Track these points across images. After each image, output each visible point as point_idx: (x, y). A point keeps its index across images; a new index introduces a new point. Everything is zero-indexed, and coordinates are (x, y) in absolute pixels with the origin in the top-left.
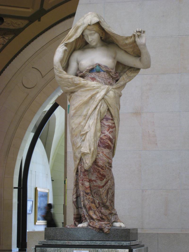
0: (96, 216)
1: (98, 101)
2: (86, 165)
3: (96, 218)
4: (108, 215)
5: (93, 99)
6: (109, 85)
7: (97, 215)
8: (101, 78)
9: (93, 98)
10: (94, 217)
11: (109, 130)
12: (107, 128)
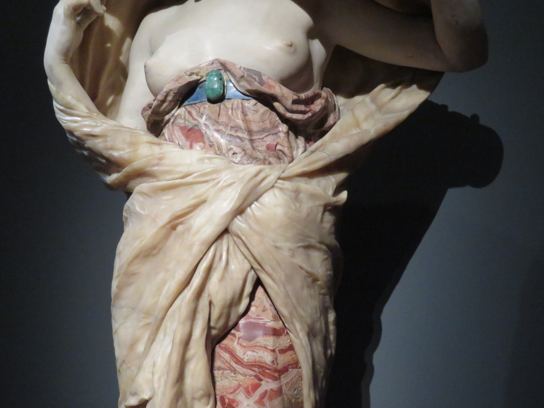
1: (196, 249)
5: (183, 233)
6: (272, 160)
8: (228, 132)
9: (180, 228)
11: (256, 387)
12: (245, 377)
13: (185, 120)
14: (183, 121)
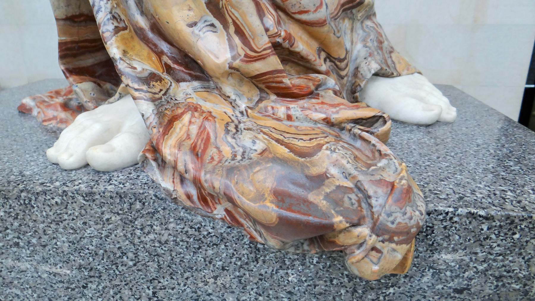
0: (237, 40)
3: (237, 63)
4: (335, 18)
7: (239, 32)
10: (215, 48)
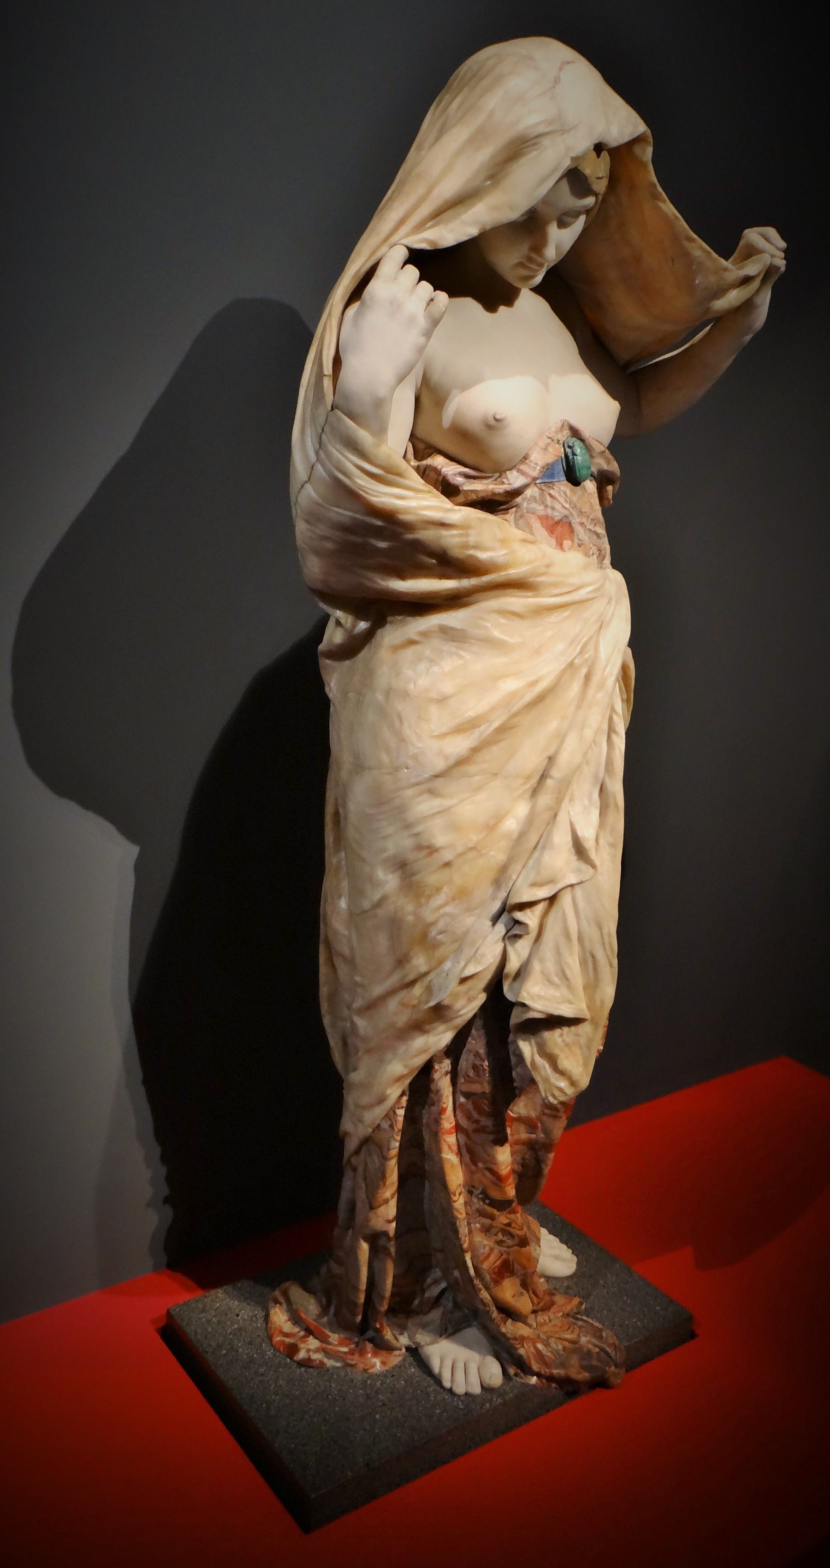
2: (563, 1084)
13: (546, 506)
14: (542, 507)
